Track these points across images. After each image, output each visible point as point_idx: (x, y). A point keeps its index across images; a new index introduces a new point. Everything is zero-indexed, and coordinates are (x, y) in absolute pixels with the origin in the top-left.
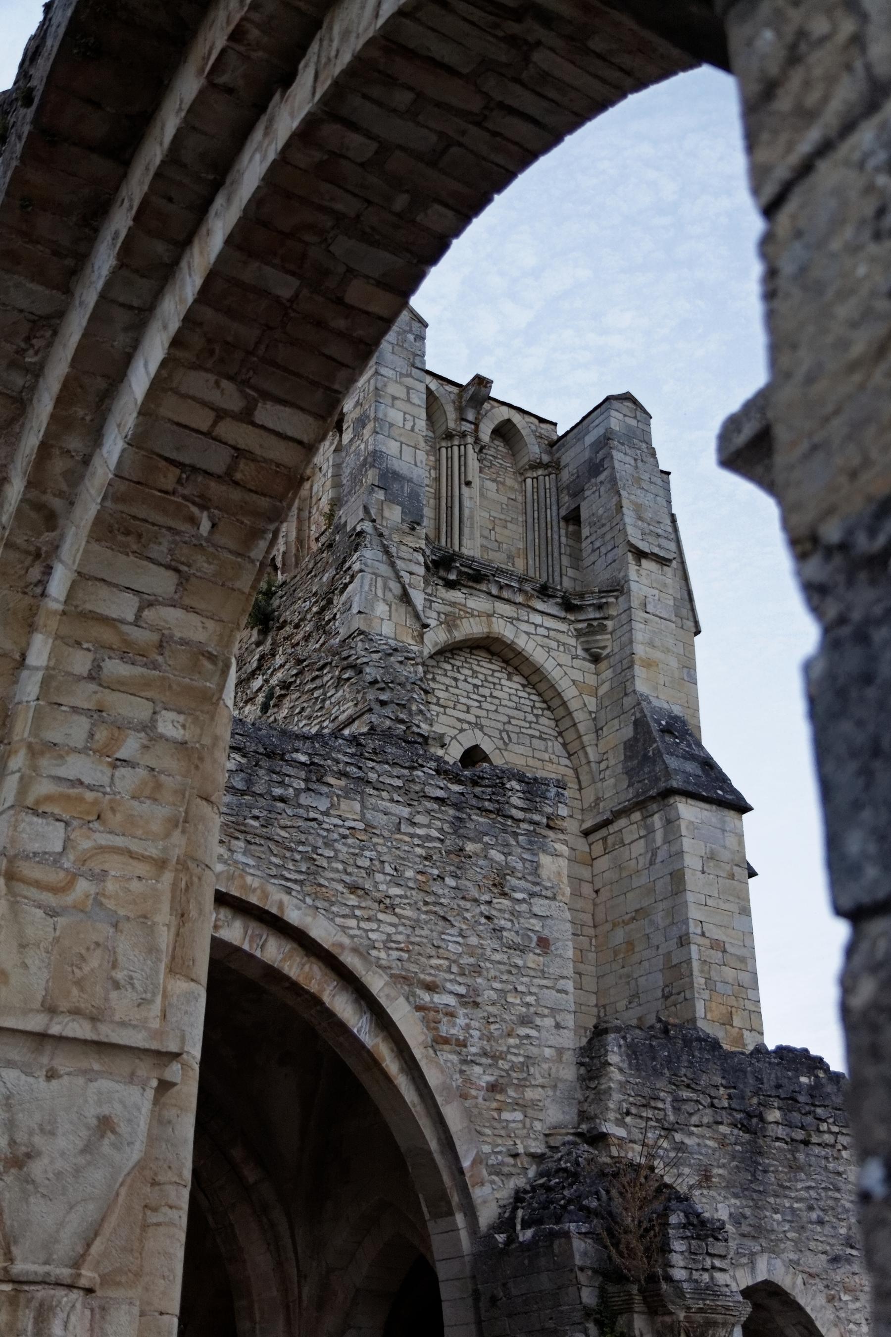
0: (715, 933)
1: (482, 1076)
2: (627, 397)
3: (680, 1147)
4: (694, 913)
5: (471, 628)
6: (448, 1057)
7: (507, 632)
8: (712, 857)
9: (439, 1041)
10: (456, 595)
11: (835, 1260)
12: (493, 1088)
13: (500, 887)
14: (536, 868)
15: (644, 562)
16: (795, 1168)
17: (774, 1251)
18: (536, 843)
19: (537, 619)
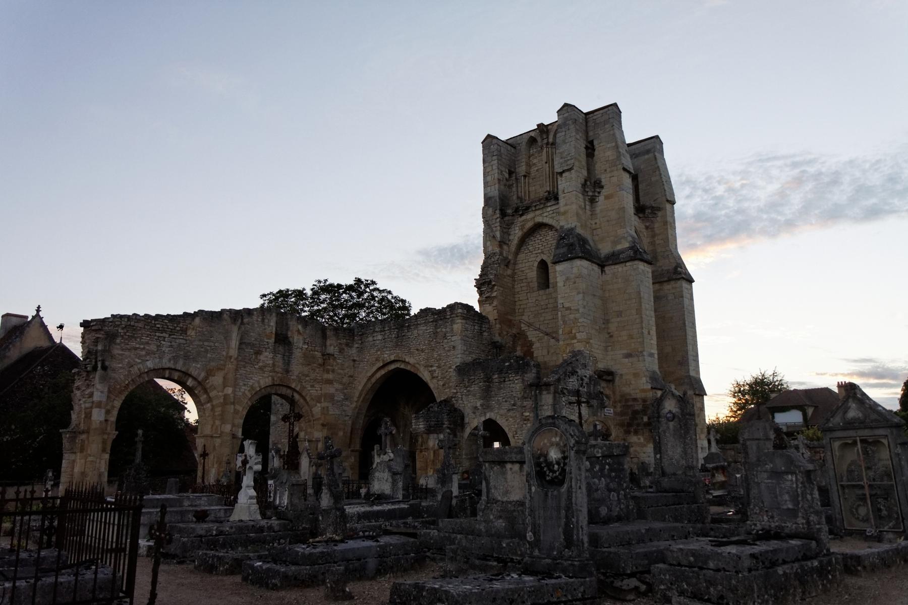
0: (567, 305)
1: (441, 383)
2: (566, 105)
3: (469, 391)
4: (560, 301)
5: (530, 224)
6: (435, 381)
7: (539, 219)
8: (568, 279)
9: (433, 378)
10: (524, 217)
11: (509, 410)
12: (444, 385)
13: (445, 337)
14: (452, 330)
15: (564, 175)
16: (500, 389)
17: (492, 410)
18: (453, 322)
19: (549, 209)
